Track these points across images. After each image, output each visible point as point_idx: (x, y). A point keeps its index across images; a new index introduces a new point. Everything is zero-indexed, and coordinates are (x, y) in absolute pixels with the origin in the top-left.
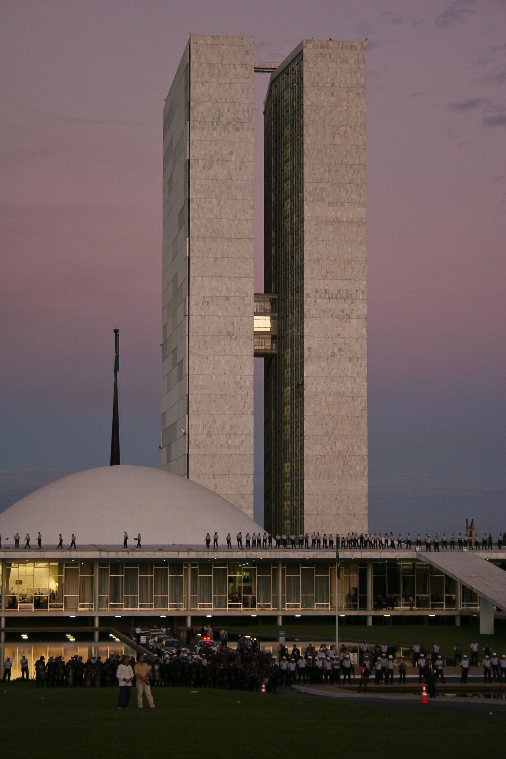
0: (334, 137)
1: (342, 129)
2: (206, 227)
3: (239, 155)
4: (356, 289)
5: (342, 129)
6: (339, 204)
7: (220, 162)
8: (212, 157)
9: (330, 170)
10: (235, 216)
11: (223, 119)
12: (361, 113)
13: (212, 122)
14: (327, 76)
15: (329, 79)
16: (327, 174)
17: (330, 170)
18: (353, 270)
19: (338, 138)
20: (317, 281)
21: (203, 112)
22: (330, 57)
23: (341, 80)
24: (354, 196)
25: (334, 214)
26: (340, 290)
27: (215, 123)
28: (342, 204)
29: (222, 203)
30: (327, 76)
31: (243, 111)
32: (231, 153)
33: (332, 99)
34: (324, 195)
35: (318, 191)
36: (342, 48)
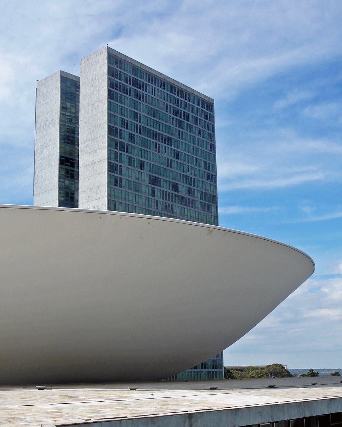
0: (92, 111)
1: (96, 104)
2: (40, 187)
3: (53, 140)
4: (102, 204)
5: (96, 104)
6: (94, 152)
7: (46, 147)
8: (43, 146)
9: (91, 132)
10: (51, 176)
11: (48, 123)
12: (105, 90)
13: (44, 127)
14: (90, 76)
15: (91, 77)
16: (89, 135)
17: (91, 132)
18: (100, 191)
19: (94, 110)
20: (84, 204)
21: (40, 122)
22: (91, 64)
23: (96, 74)
24: (101, 144)
25: (92, 159)
26: (95, 206)
27: (45, 126)
28: (96, 152)
29: (46, 171)
30: (90, 76)
31: (55, 114)
32: (50, 141)
33: (92, 88)
34: (88, 148)
35: (85, 148)
36: (97, 56)
